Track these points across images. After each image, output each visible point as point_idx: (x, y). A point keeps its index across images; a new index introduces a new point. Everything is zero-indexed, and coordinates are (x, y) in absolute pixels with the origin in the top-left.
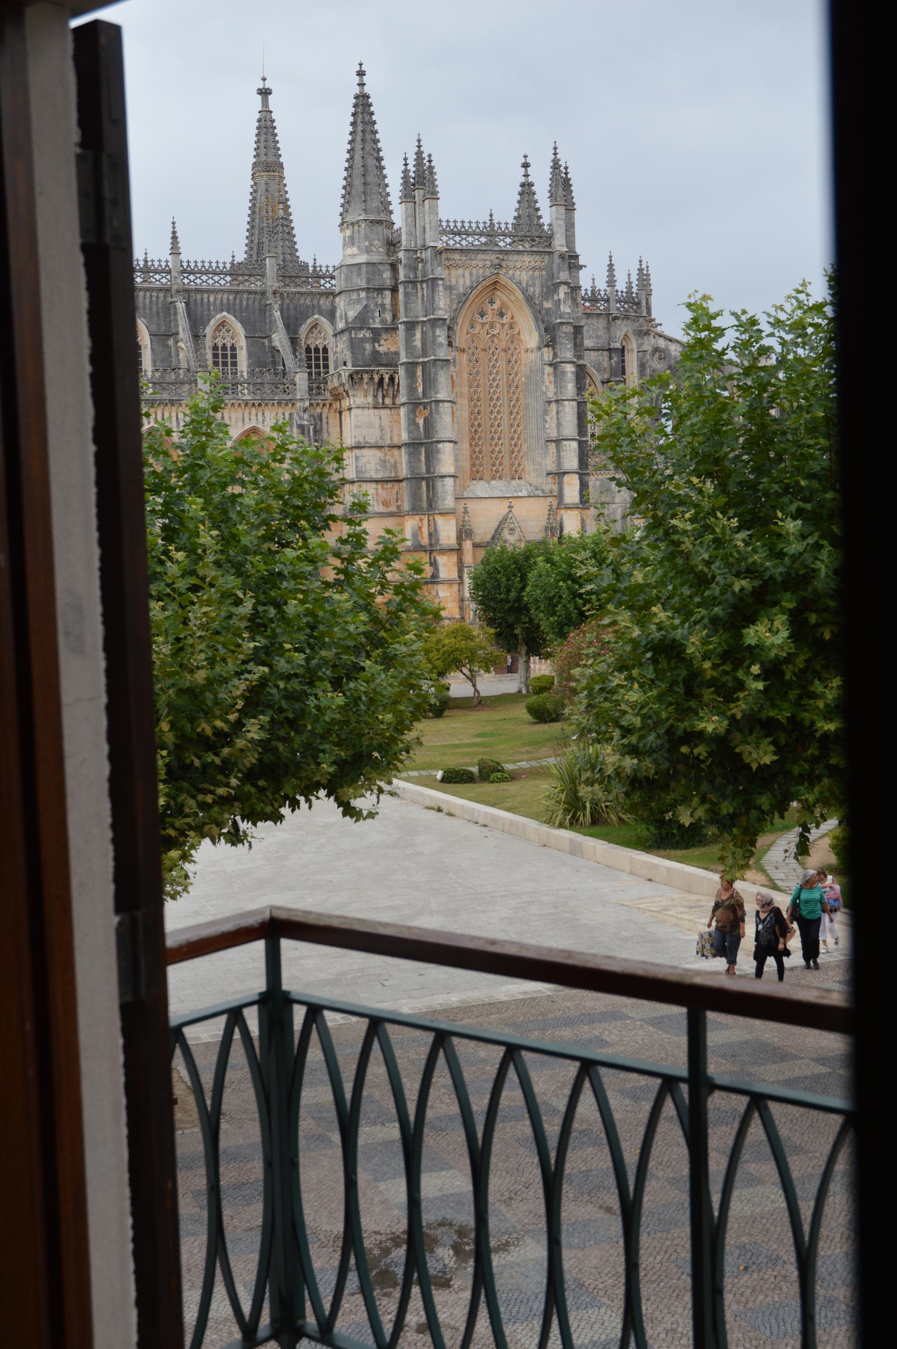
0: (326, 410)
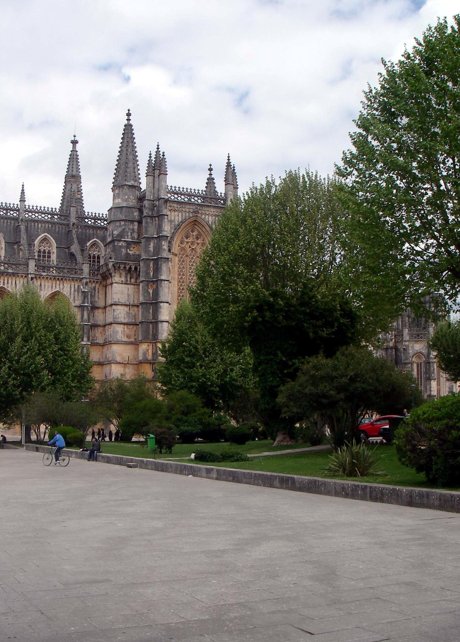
0: (97, 286)
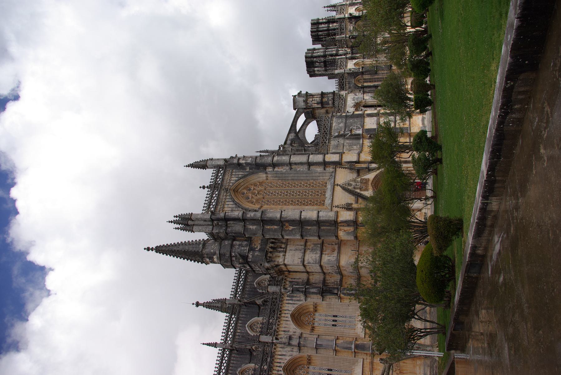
0: (288, 279)
